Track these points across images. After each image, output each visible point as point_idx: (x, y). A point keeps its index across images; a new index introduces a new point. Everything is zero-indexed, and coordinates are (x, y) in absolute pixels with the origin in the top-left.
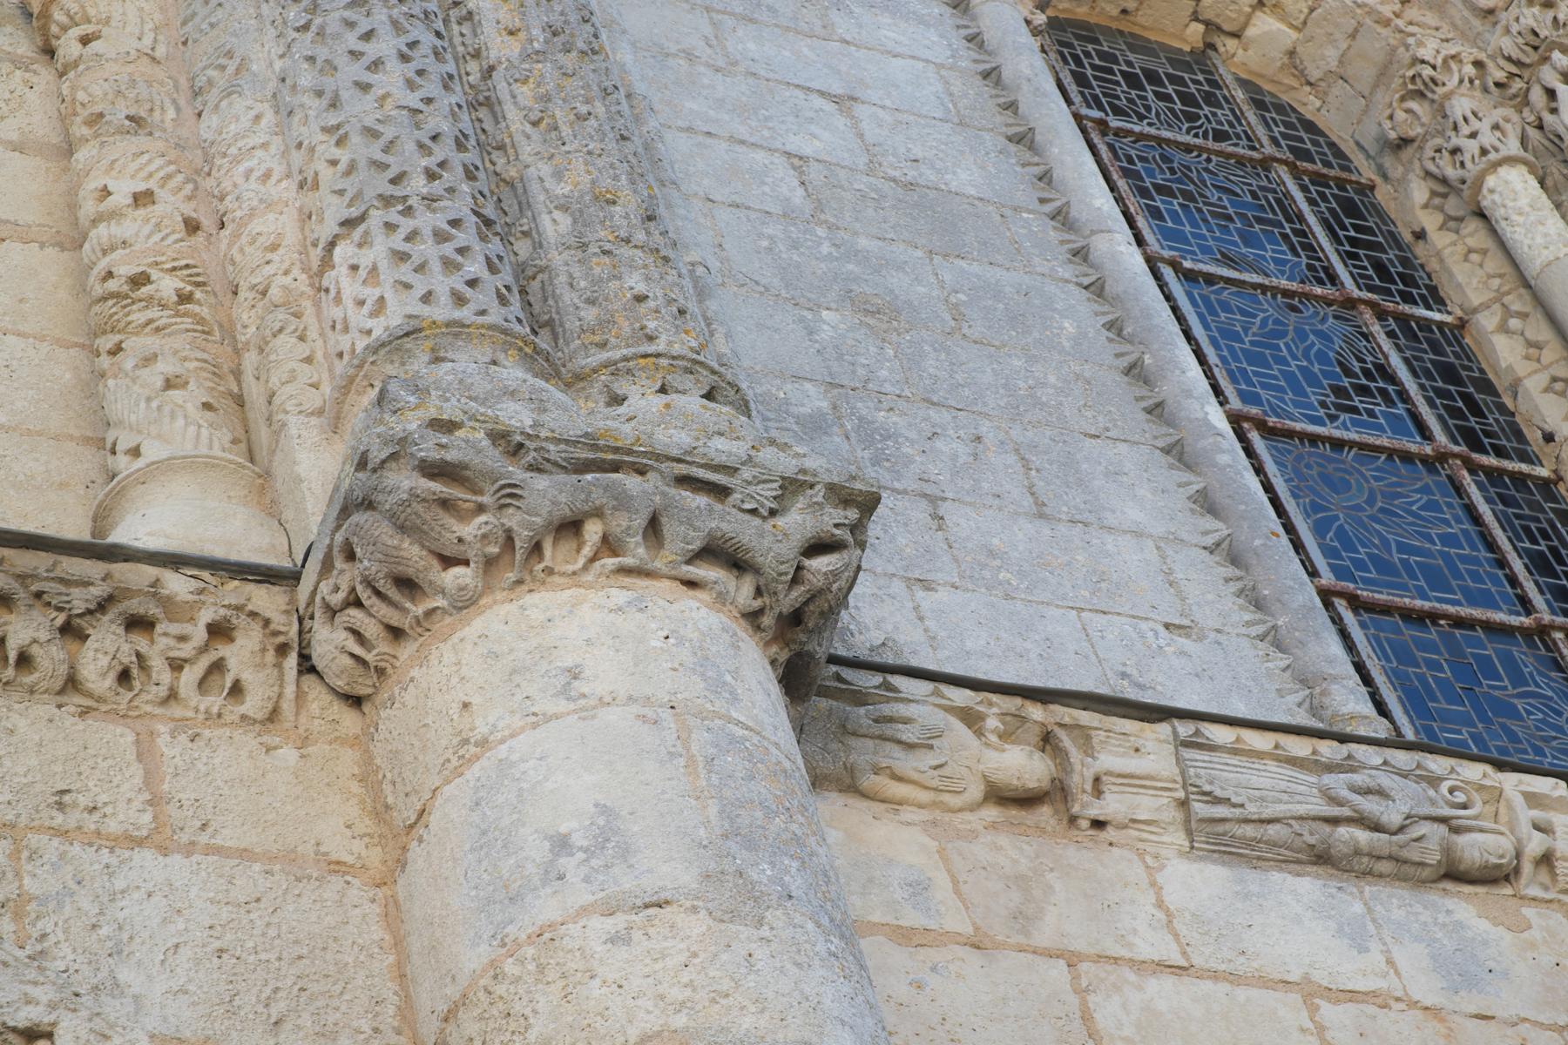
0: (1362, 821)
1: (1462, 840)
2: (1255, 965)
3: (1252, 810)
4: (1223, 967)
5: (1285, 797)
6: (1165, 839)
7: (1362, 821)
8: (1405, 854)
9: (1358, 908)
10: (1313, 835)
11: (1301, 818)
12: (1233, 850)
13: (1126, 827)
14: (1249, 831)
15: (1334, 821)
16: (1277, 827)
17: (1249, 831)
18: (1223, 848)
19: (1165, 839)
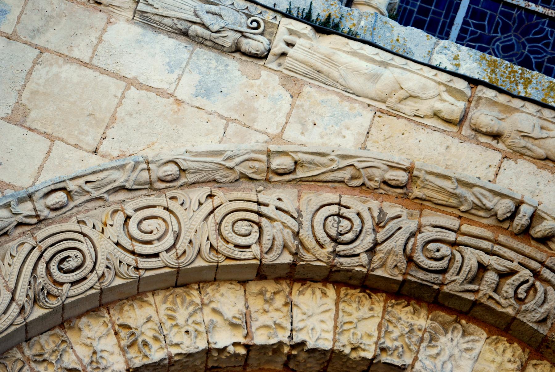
0: (203, 25)
1: (244, 41)
2: (118, 68)
3: (161, 11)
4: (103, 66)
5: (177, 9)
6: (123, 13)
7: (203, 25)
8: (216, 41)
9: (186, 55)
10: (182, 26)
11: (179, 19)
12: (149, 23)
13: (108, 6)
14: (157, 18)
15: (194, 23)
16: (169, 19)
17: (157, 18)
18: (145, 22)
19: (123, 13)
